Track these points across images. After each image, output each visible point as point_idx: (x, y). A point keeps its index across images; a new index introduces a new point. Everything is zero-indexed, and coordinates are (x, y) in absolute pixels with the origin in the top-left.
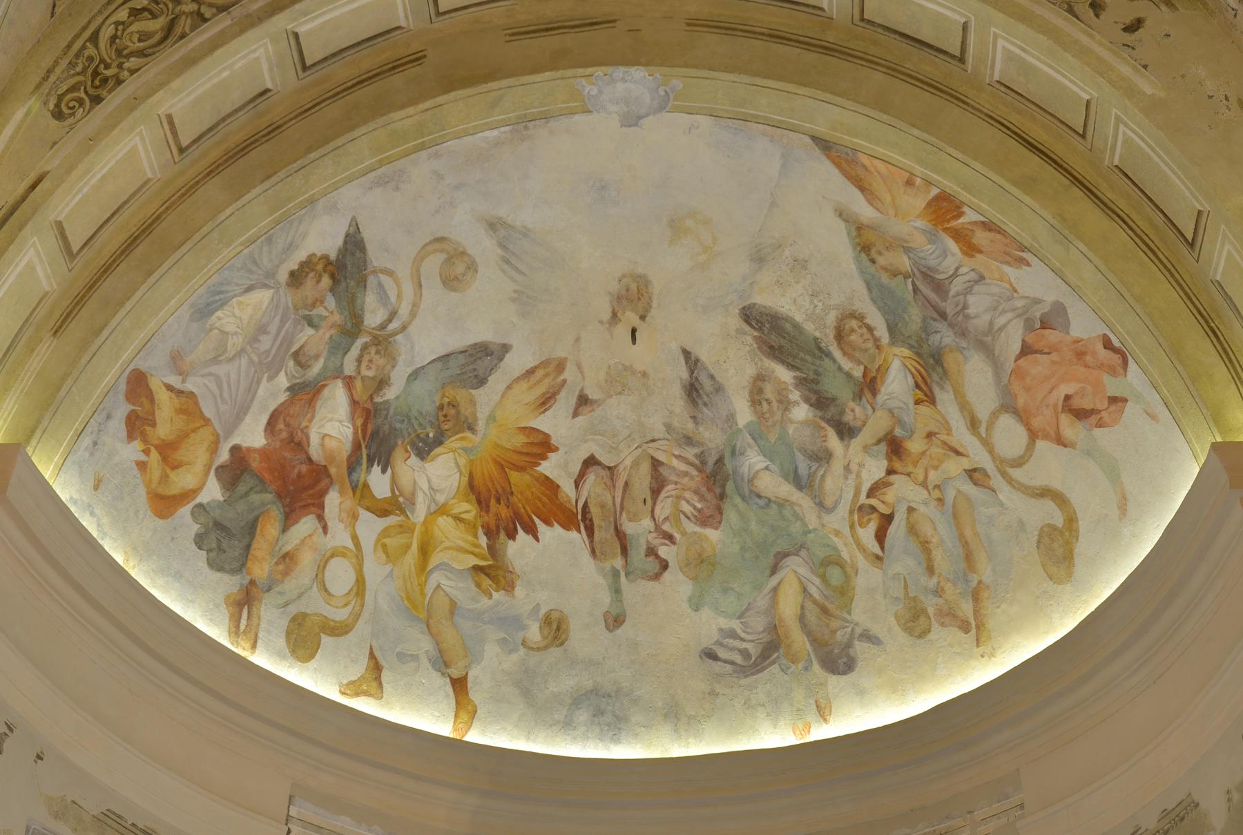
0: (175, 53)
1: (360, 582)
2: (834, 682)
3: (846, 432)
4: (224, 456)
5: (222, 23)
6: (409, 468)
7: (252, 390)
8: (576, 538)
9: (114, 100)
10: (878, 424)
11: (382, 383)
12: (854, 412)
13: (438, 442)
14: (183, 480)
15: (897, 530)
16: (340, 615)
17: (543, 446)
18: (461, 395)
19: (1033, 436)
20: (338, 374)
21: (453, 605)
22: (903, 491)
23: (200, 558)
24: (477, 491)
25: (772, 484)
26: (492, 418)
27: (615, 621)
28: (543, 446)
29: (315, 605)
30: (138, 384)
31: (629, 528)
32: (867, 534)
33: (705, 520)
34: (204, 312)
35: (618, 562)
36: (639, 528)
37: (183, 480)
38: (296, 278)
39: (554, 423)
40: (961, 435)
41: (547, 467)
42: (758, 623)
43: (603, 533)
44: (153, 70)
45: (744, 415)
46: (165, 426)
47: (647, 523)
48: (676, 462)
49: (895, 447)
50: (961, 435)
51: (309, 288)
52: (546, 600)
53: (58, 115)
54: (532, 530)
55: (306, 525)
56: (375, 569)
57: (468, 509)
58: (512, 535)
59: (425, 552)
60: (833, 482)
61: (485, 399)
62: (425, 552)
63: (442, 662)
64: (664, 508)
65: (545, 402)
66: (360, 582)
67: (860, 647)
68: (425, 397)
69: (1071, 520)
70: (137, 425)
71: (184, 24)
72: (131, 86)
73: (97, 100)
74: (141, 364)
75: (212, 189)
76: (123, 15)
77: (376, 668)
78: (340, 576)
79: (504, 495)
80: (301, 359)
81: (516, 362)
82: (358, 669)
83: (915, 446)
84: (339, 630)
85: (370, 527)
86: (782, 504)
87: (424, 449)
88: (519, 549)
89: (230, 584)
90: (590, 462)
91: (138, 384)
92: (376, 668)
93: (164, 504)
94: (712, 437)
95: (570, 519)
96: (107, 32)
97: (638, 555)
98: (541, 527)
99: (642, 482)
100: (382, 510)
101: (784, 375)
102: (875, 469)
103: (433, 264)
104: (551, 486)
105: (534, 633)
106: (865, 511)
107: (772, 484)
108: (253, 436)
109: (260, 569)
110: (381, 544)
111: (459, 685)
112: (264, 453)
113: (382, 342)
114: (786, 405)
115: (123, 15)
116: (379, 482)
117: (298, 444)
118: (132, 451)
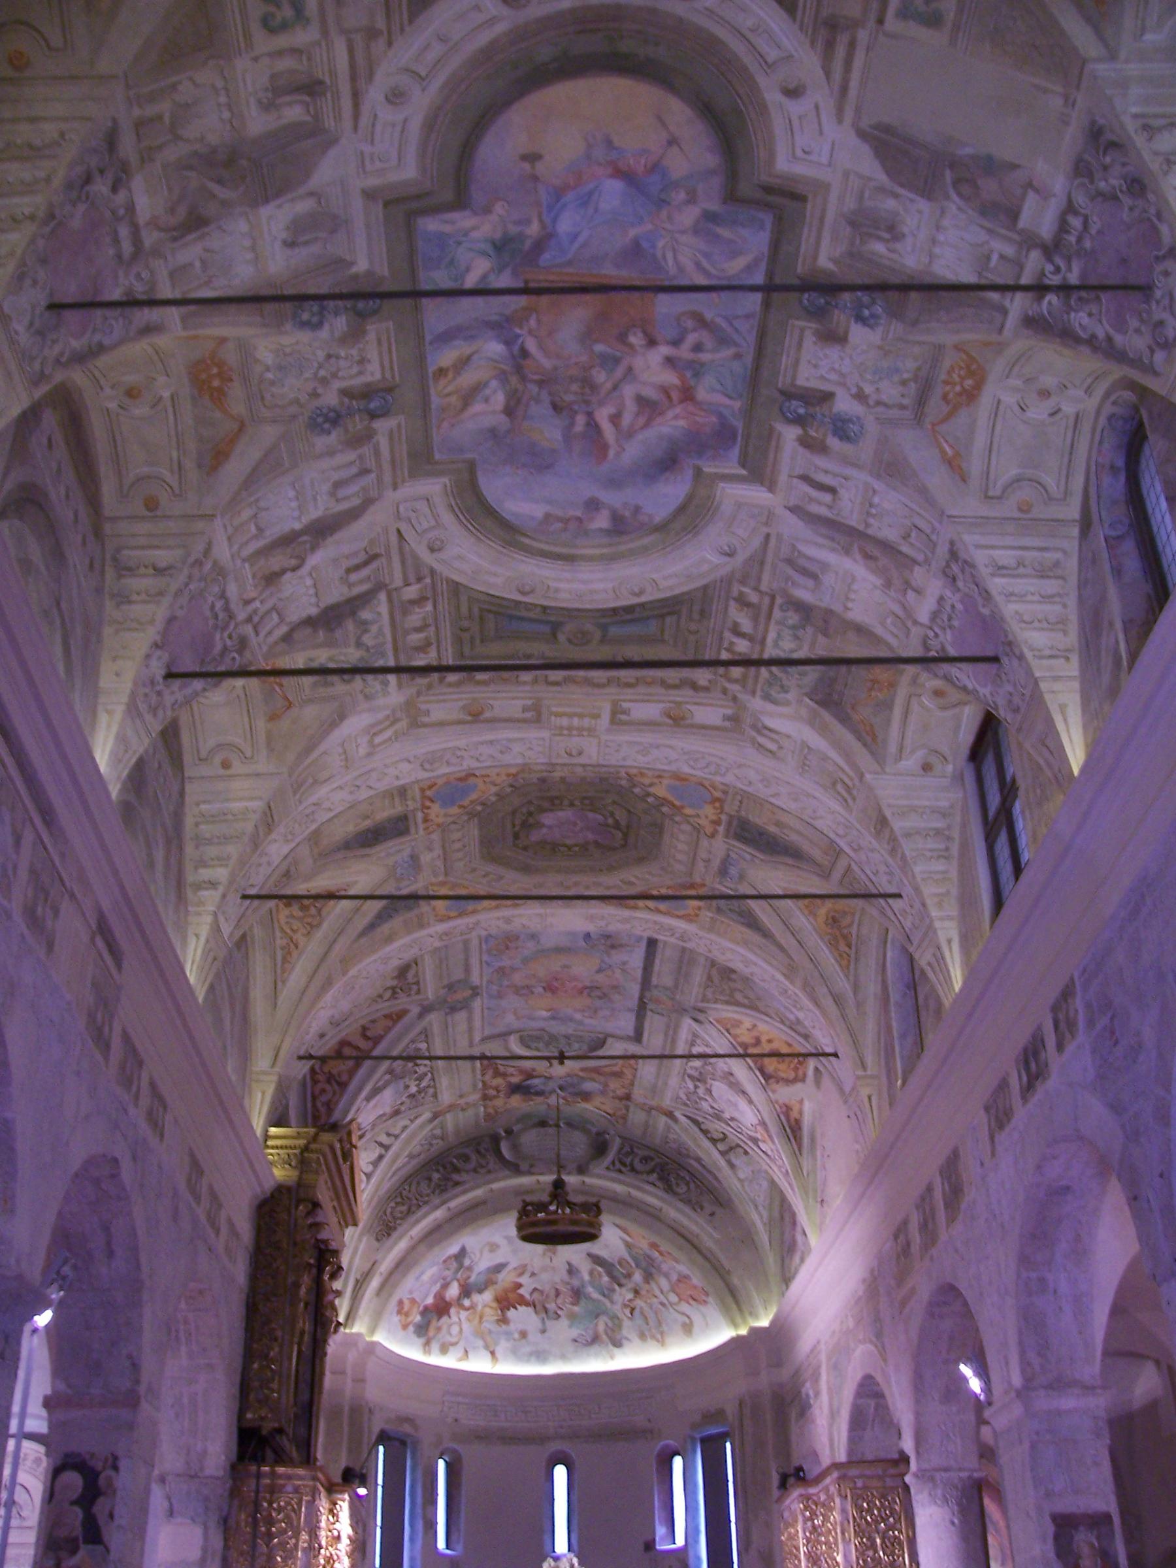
1: (461, 1330)
2: (616, 1350)
3: (620, 1285)
4: (421, 1308)
5: (425, 1209)
8: (530, 1310)
9: (395, 1235)
10: (630, 1285)
11: (469, 1277)
12: (623, 1281)
13: (486, 1288)
14: (410, 1319)
15: (636, 1313)
16: (454, 1340)
17: (520, 1286)
19: (680, 1300)
21: (490, 1332)
22: (639, 1303)
23: (414, 1337)
24: (498, 1300)
25: (595, 1295)
27: (543, 1331)
28: (520, 1286)
31: (548, 1306)
32: (627, 1312)
33: (573, 1304)
34: (417, 1278)
35: (544, 1315)
36: (551, 1306)
38: (445, 1261)
39: (524, 1280)
40: (657, 1292)
41: (521, 1291)
42: (591, 1332)
43: (539, 1307)
44: (405, 1226)
45: (587, 1277)
47: (553, 1305)
48: (563, 1289)
49: (637, 1292)
50: (657, 1292)
52: (521, 1327)
53: (378, 1240)
54: (515, 1308)
55: (445, 1319)
56: (466, 1326)
57: (495, 1305)
59: (481, 1318)
60: (616, 1297)
61: (501, 1276)
62: (481, 1318)
63: (486, 1347)
64: (559, 1301)
65: (521, 1274)
66: (461, 1330)
67: (624, 1342)
68: (483, 1278)
69: (691, 1323)
70: (399, 1312)
71: (413, 1209)
72: (400, 1230)
73: (389, 1235)
75: (422, 1248)
76: (393, 1204)
77: (466, 1352)
78: (455, 1330)
79: (507, 1299)
80: (444, 1279)
81: (510, 1267)
82: (461, 1353)
83: (643, 1292)
84: (454, 1344)
86: (599, 1301)
87: (480, 1291)
88: (511, 1313)
89: (422, 1340)
90: (535, 1289)
91: (401, 1303)
92: (466, 1352)
93: (405, 1327)
94: (576, 1282)
95: (527, 1304)
96: (389, 1210)
97: (551, 1314)
99: (553, 1293)
100: (467, 1309)
101: (600, 1269)
102: (630, 1296)
103: (487, 1249)
104: (522, 1296)
105: (516, 1336)
106: (625, 1306)
107: (595, 1295)
109: (431, 1333)
113: (470, 1269)
114: (600, 1275)
115: (393, 1204)
116: (467, 1303)
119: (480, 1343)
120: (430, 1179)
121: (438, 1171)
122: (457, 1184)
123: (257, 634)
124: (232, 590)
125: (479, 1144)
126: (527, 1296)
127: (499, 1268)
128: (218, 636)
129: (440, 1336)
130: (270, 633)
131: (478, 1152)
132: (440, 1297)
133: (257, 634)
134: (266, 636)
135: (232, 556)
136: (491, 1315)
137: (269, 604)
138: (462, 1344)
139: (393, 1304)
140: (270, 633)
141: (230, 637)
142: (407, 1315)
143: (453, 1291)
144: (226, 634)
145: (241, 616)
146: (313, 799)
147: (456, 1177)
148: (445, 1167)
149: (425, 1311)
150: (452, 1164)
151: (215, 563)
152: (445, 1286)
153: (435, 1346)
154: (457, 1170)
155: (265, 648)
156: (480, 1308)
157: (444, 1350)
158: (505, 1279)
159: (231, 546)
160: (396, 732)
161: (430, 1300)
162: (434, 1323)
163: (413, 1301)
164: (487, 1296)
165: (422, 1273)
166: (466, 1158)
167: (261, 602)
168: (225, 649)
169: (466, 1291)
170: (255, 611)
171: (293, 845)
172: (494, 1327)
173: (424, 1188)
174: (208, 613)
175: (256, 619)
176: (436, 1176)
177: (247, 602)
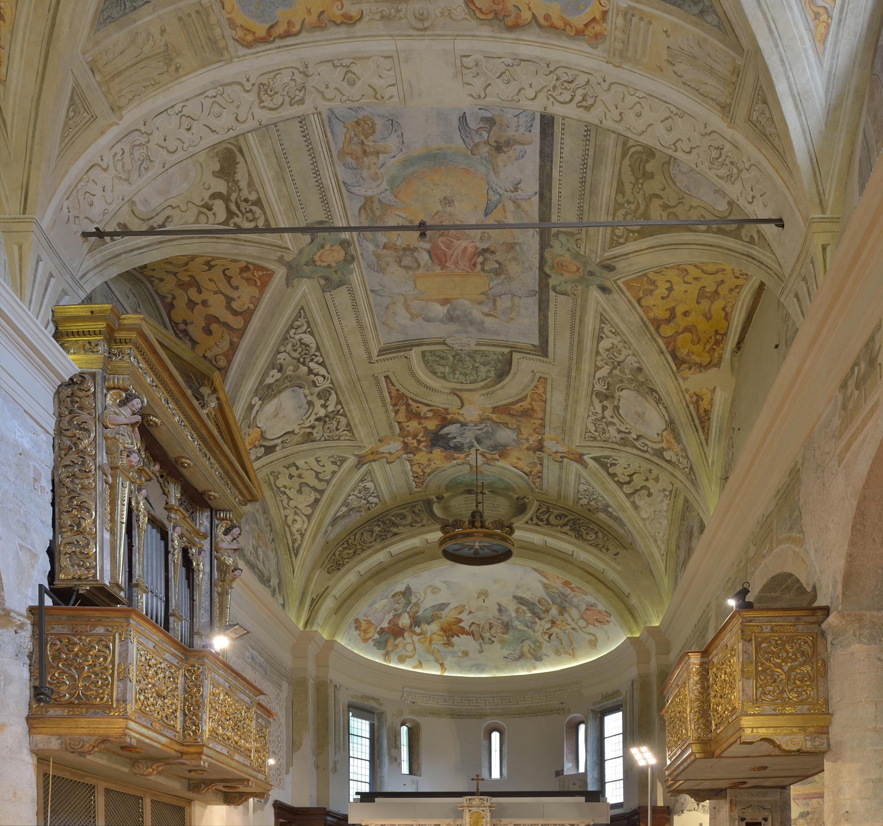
0: (358, 558)
1: (415, 649)
2: (537, 662)
4: (378, 629)
6: (425, 627)
7: (384, 617)
9: (343, 570)
11: (417, 612)
13: (433, 621)
14: (368, 636)
17: (461, 621)
18: (438, 613)
20: (406, 611)
24: (442, 629)
25: (521, 627)
26: (446, 616)
28: (461, 621)
29: (404, 653)
30: (357, 621)
31: (484, 635)
35: (481, 641)
36: (487, 635)
37: (368, 636)
38: (393, 596)
41: (461, 624)
42: (518, 652)
44: (352, 563)
46: (364, 626)
47: (489, 634)
51: (397, 597)
52: (463, 649)
54: (458, 636)
55: (400, 639)
56: (418, 645)
57: (442, 633)
58: (453, 637)
59: (430, 641)
62: (430, 641)
63: (437, 661)
64: (493, 631)
65: (460, 613)
66: (415, 649)
68: (428, 614)
70: (357, 628)
71: (359, 551)
73: (339, 569)
74: (357, 617)
78: (410, 648)
81: (452, 606)
82: (416, 663)
85: (416, 638)
86: (524, 631)
87: (429, 623)
88: (455, 639)
89: (383, 652)
91: (357, 621)
93: (365, 640)
94: (505, 619)
97: (486, 640)
98: (460, 635)
99: (487, 626)
100: (419, 635)
103: (429, 590)
104: (463, 628)
105: (460, 654)
108: (385, 625)
109: (389, 648)
110: (419, 640)
111: (442, 665)
112: (388, 628)
113: (416, 605)
116: (418, 630)
117: (397, 625)
118: (357, 632)
119: (432, 658)
120: (372, 531)
121: (379, 526)
122: (395, 534)
125: (414, 506)
126: (467, 628)
127: (442, 606)
129: (397, 650)
131: (414, 512)
132: (393, 623)
136: (438, 641)
138: (416, 656)
139: (350, 619)
142: (365, 631)
143: (405, 621)
147: (394, 530)
148: (384, 523)
149: (382, 631)
150: (390, 520)
152: (398, 616)
153: (393, 656)
154: (394, 524)
156: (429, 634)
157: (401, 660)
158: (448, 615)
161: (385, 625)
162: (391, 641)
163: (369, 623)
164: (434, 627)
165: (374, 602)
166: (404, 517)
169: (416, 622)
172: (441, 648)
173: (367, 537)
176: (377, 529)
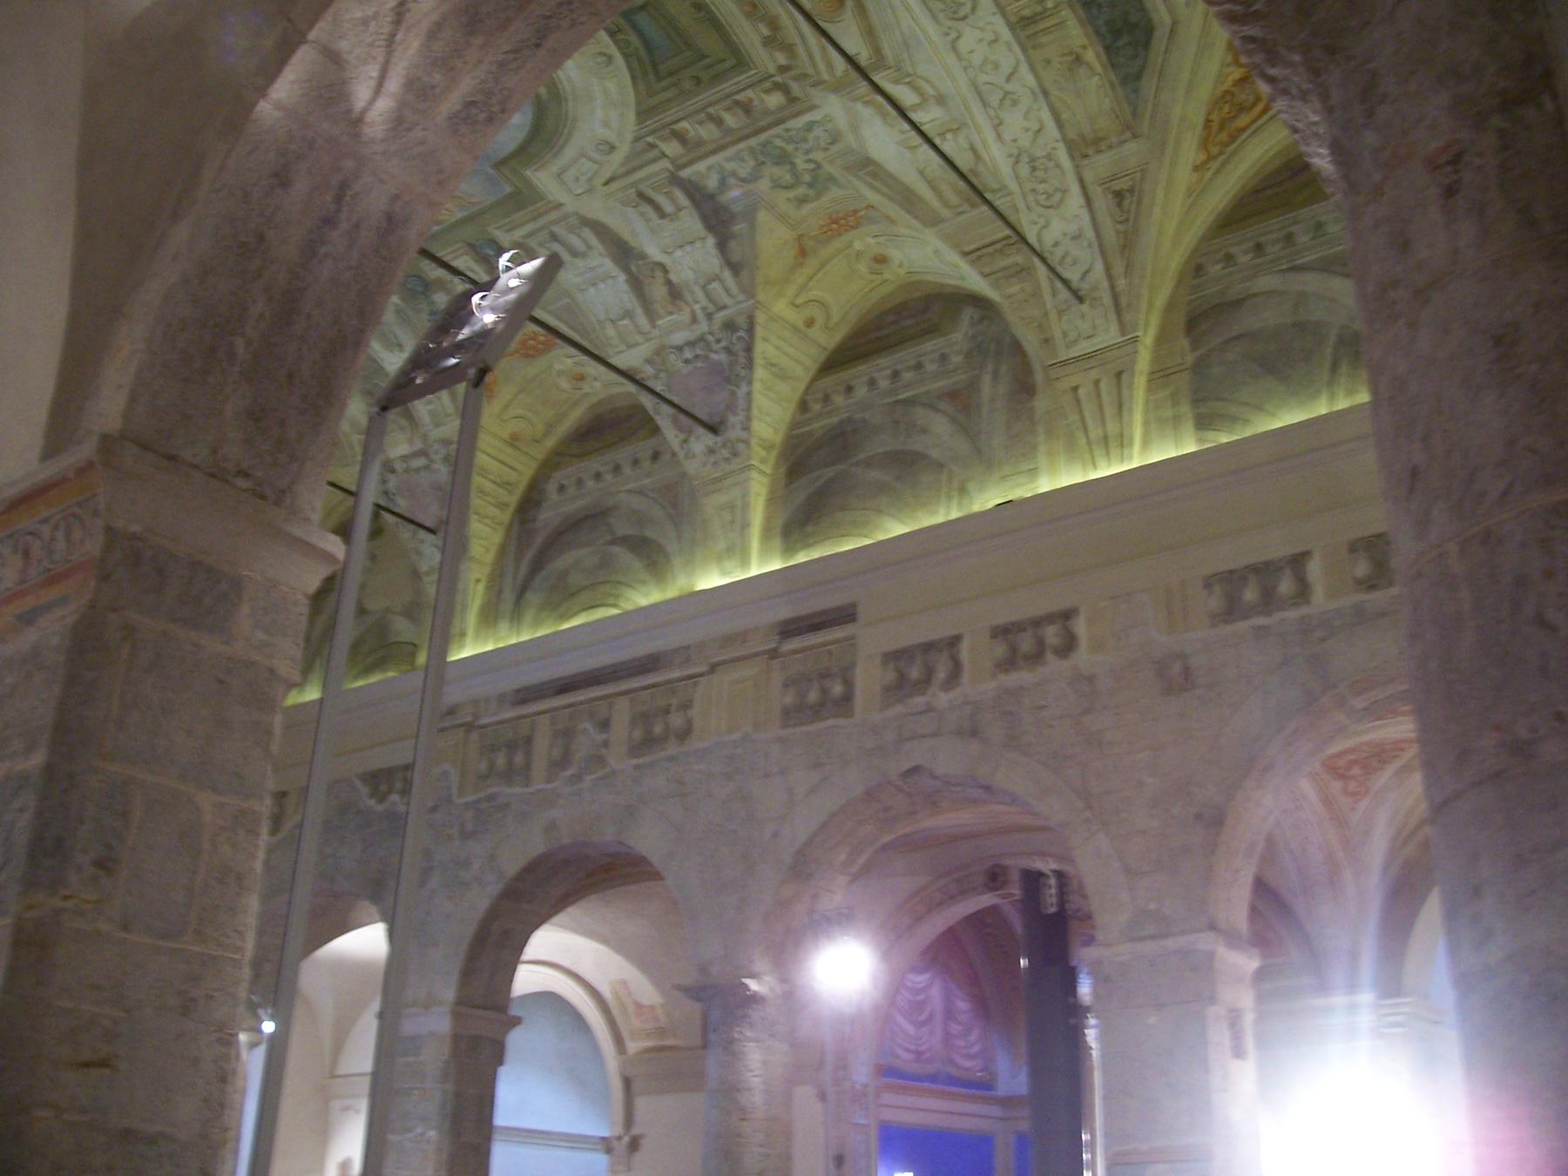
123: (725, 307)
124: (679, 338)
128: (714, 356)
130: (727, 291)
133: (725, 307)
134: (730, 295)
135: (648, 340)
137: (700, 294)
140: (727, 291)
141: (718, 341)
144: (716, 347)
145: (703, 327)
146: (1005, 168)
151: (649, 361)
155: (742, 297)
159: (637, 344)
160: (896, 82)
167: (697, 302)
168: (728, 350)
170: (704, 309)
171: (1075, 189)
174: (690, 367)
175: (711, 308)
177: (694, 320)
